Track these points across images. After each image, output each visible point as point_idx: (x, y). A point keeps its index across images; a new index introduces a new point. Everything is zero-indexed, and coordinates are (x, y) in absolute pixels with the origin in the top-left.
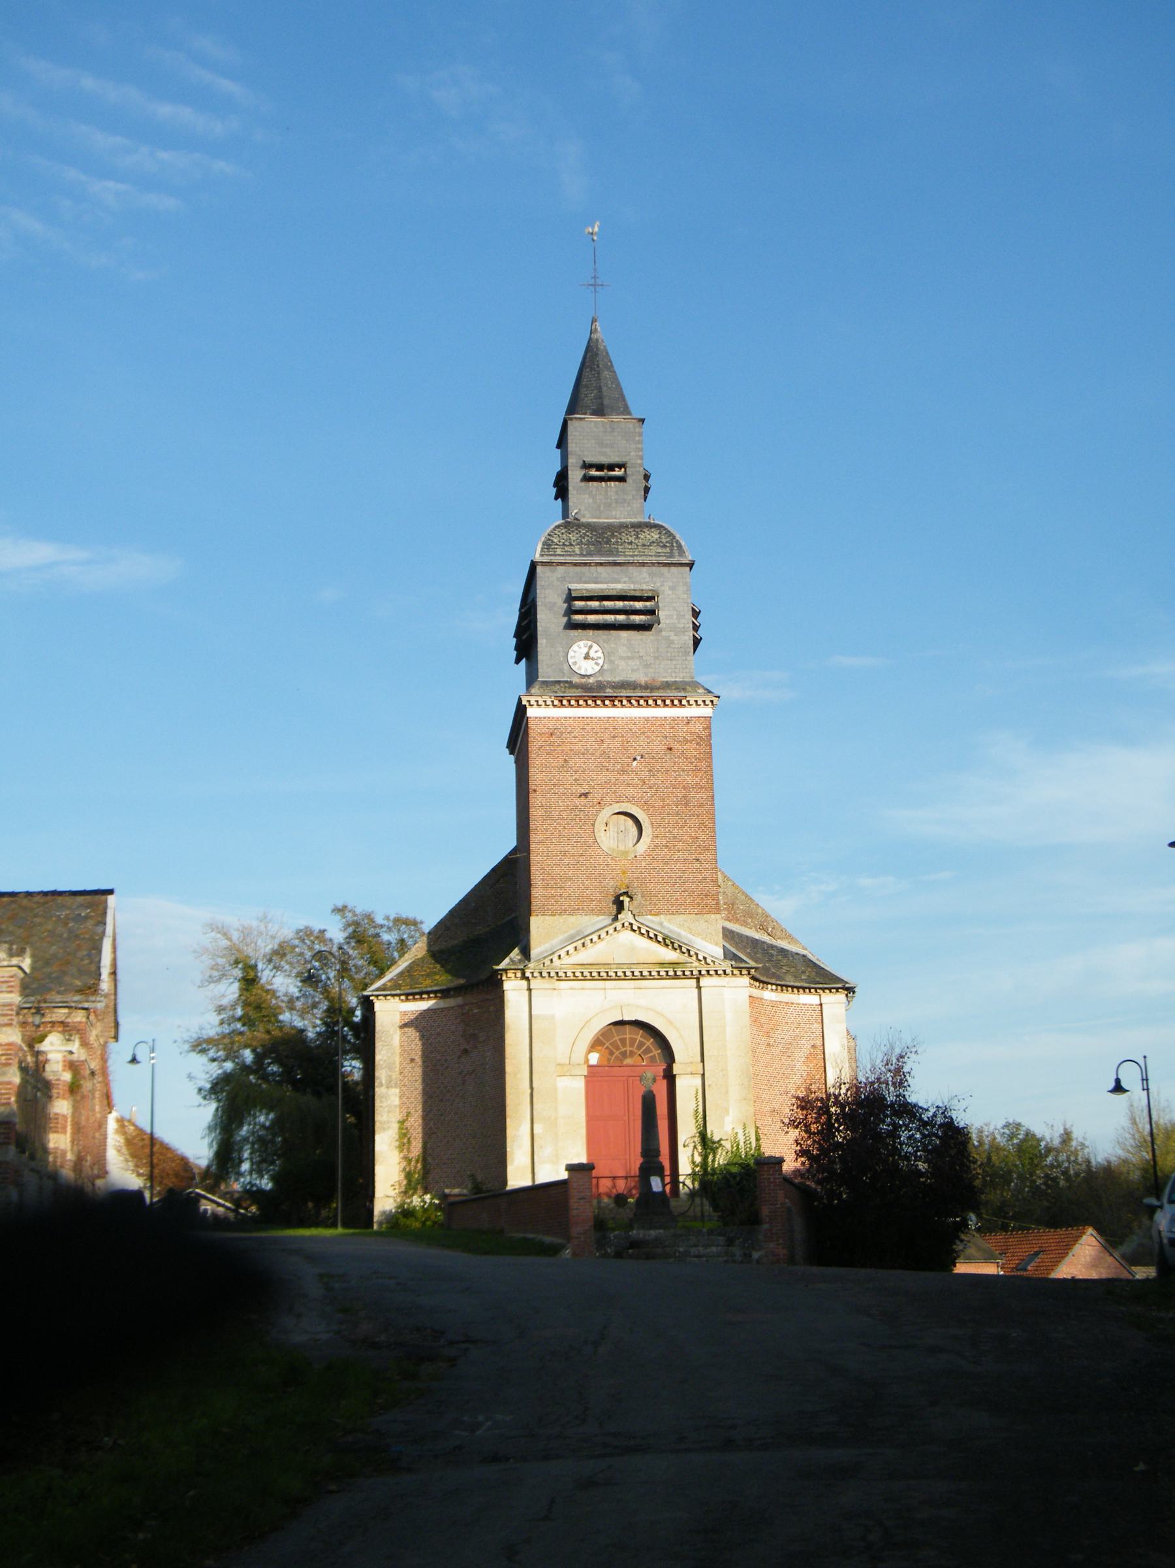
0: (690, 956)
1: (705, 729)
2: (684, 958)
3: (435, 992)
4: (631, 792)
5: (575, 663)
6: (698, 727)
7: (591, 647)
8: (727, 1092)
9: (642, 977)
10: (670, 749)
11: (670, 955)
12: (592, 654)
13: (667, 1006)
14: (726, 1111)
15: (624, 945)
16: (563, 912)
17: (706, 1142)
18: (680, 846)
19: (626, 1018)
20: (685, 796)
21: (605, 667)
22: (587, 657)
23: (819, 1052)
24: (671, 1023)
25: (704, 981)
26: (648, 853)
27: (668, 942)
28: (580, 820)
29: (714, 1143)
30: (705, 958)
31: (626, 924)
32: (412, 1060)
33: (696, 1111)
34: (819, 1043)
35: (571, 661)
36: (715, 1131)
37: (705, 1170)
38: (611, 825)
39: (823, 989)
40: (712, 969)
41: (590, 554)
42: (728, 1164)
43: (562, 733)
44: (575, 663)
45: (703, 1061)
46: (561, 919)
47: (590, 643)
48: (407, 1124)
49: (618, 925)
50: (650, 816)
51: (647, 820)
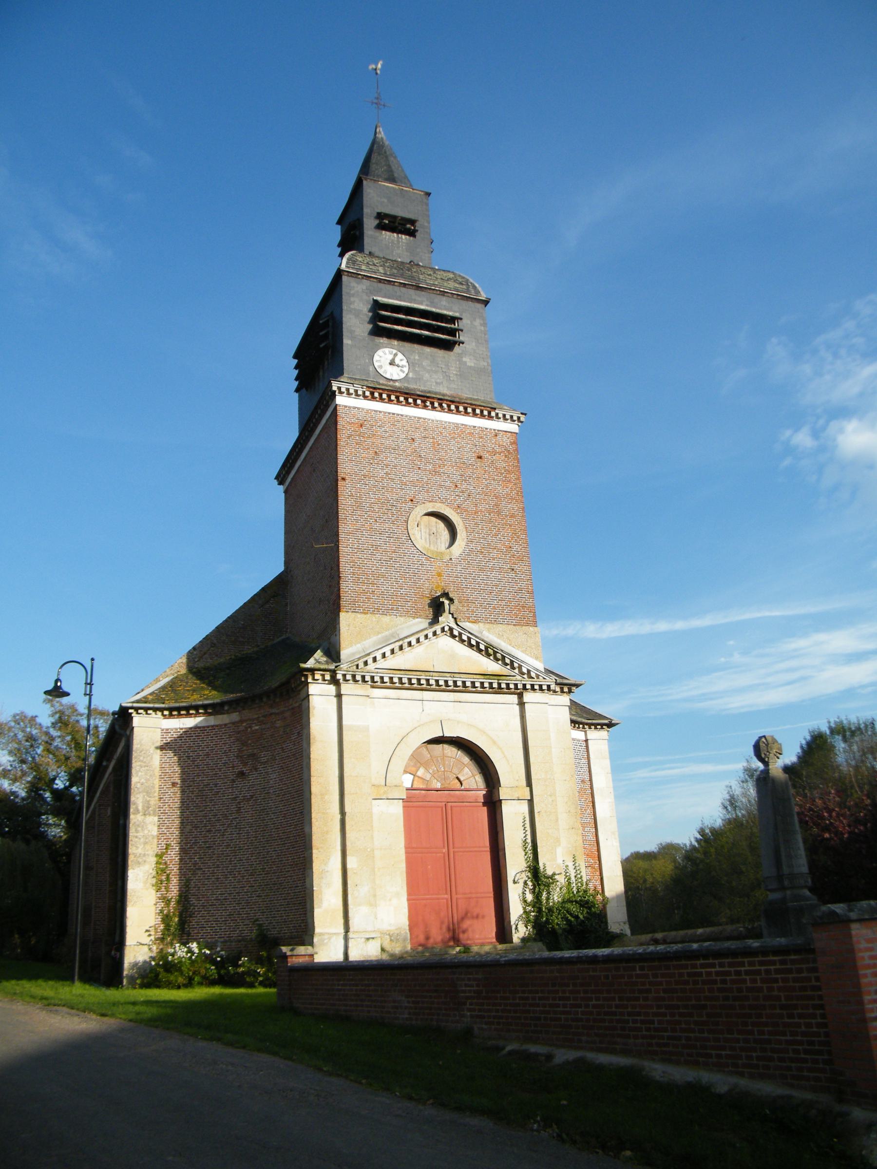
0: (513, 668)
1: (512, 444)
2: (505, 671)
3: (205, 707)
4: (443, 493)
5: (381, 367)
6: (506, 441)
7: (396, 355)
8: (557, 820)
9: (465, 689)
10: (480, 457)
11: (494, 667)
12: (397, 361)
13: (488, 720)
14: (558, 841)
15: (443, 653)
16: (376, 611)
17: (537, 876)
18: (494, 553)
19: (448, 734)
20: (497, 505)
21: (411, 375)
22: (392, 363)
23: (588, 786)
24: (494, 742)
25: (528, 697)
26: (468, 554)
27: (490, 651)
28: (393, 515)
29: (548, 878)
30: (529, 671)
31: (447, 629)
32: (174, 784)
33: (525, 842)
34: (587, 778)
35: (376, 364)
36: (549, 864)
37: (540, 910)
38: (422, 526)
39: (590, 725)
40: (537, 683)
41: (392, 275)
42: (563, 902)
43: (372, 426)
44: (381, 367)
45: (529, 784)
46: (375, 618)
47: (395, 351)
48: (166, 858)
49: (438, 628)
50: (464, 520)
51: (461, 524)
